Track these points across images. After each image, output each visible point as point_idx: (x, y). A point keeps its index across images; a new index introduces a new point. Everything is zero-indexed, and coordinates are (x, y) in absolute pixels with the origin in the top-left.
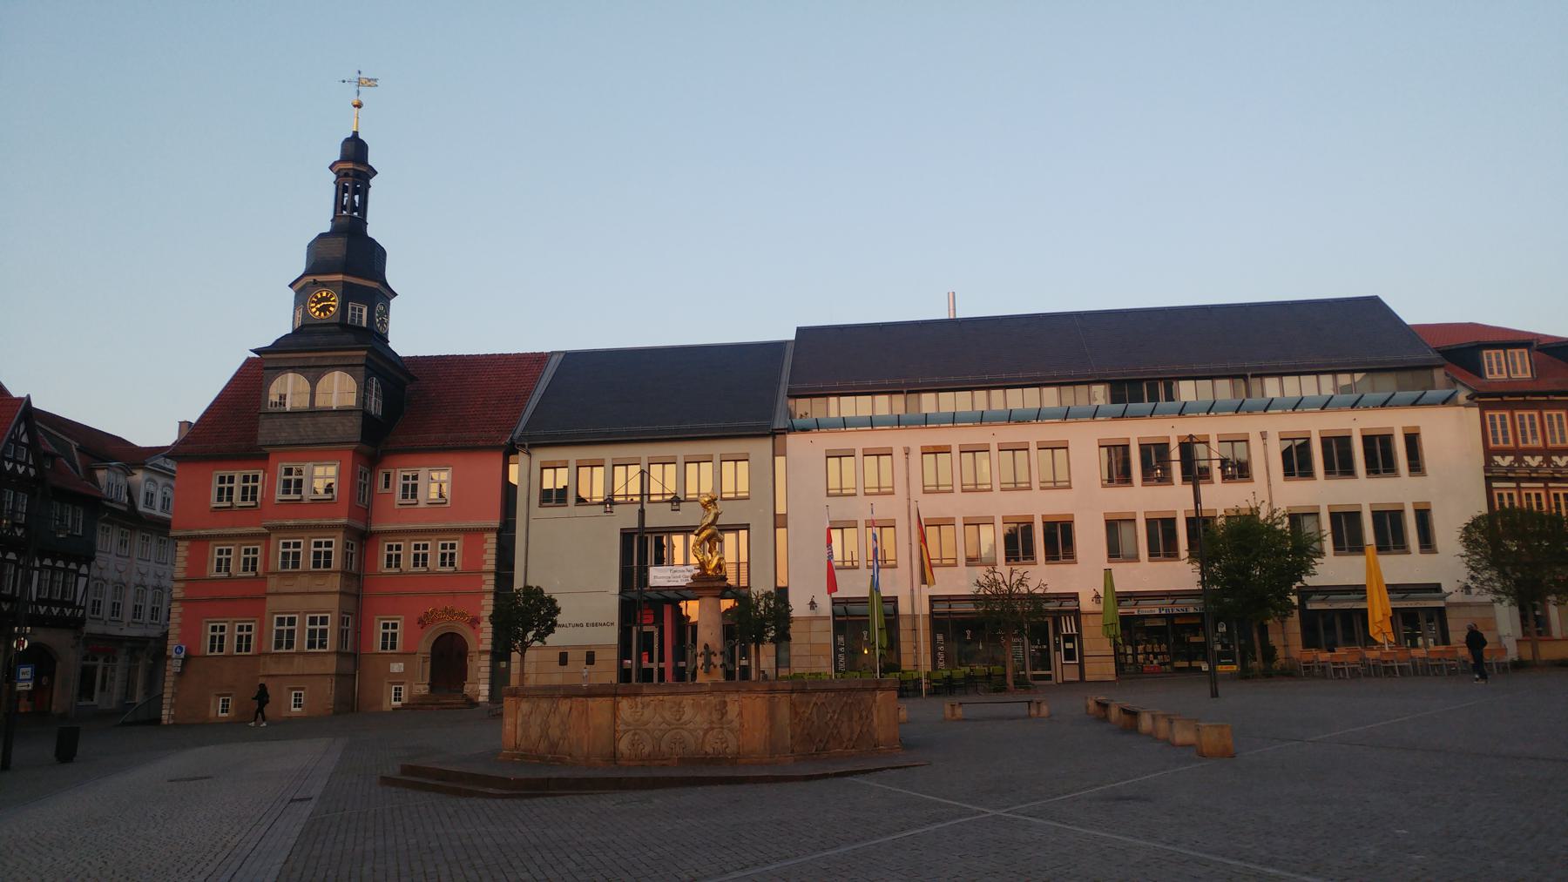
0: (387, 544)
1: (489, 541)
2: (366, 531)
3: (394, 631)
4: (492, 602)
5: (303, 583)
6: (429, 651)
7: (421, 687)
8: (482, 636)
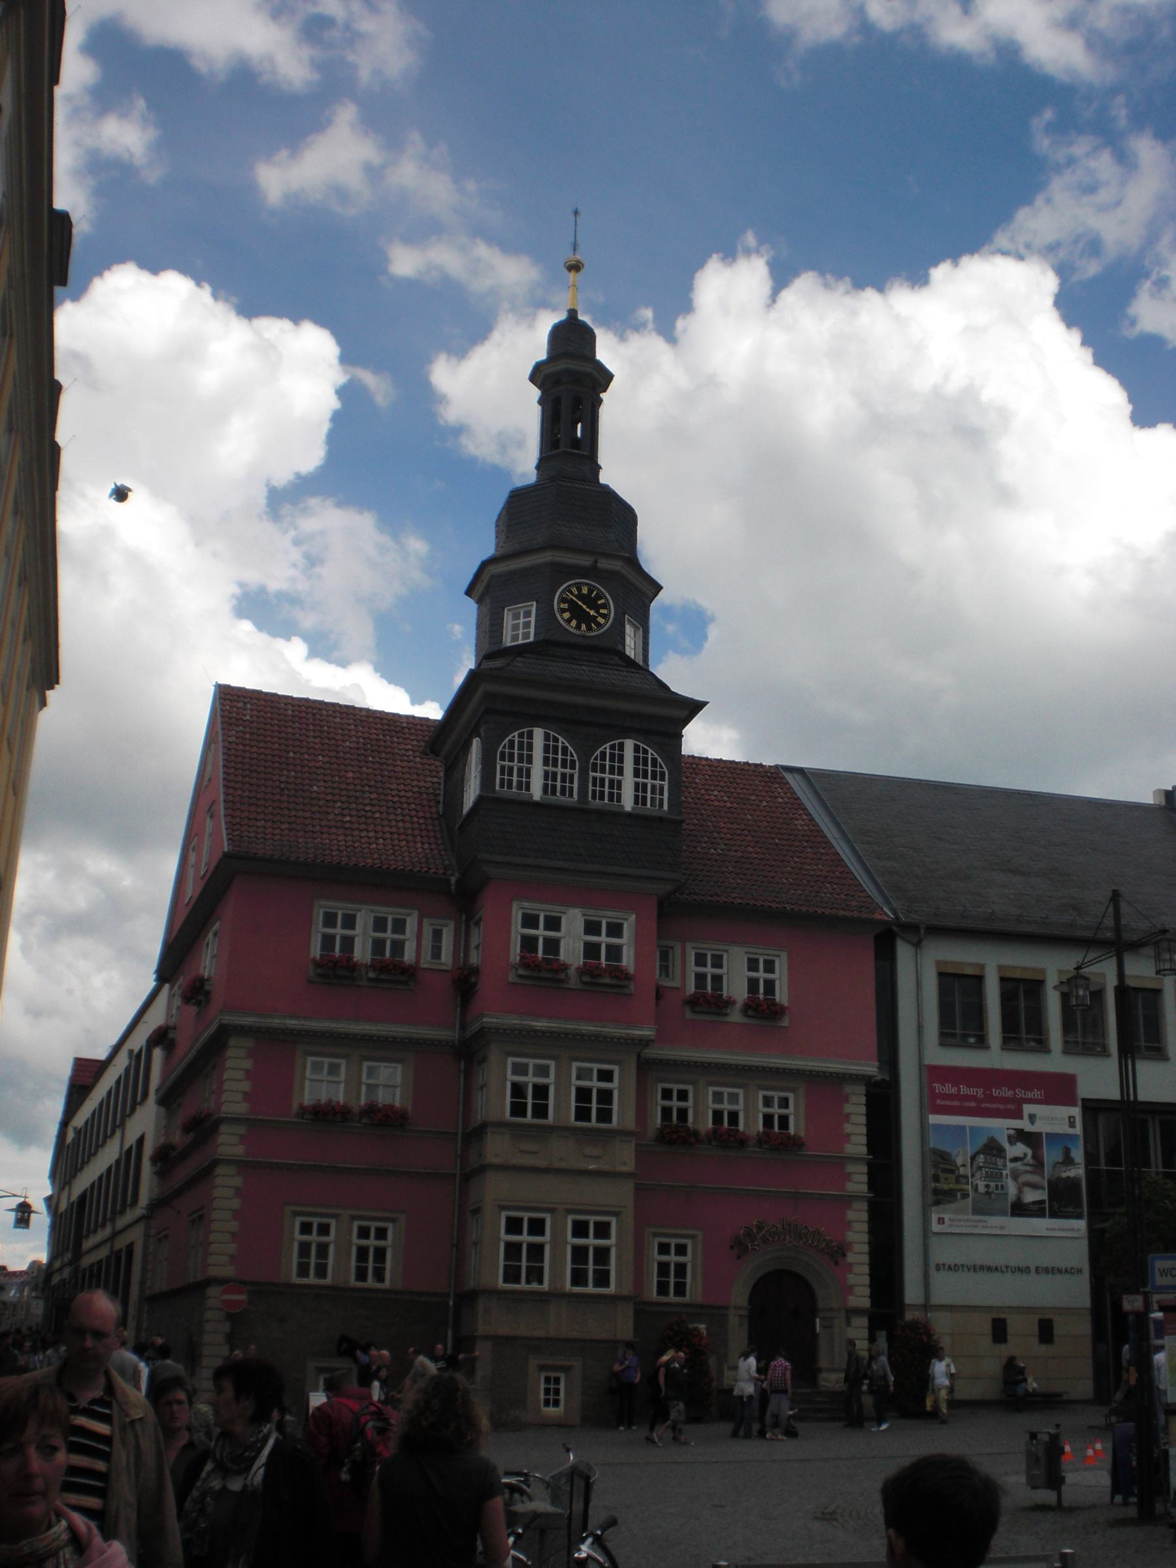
0: (660, 1086)
1: (854, 1099)
5: (563, 1152)
8: (852, 1279)
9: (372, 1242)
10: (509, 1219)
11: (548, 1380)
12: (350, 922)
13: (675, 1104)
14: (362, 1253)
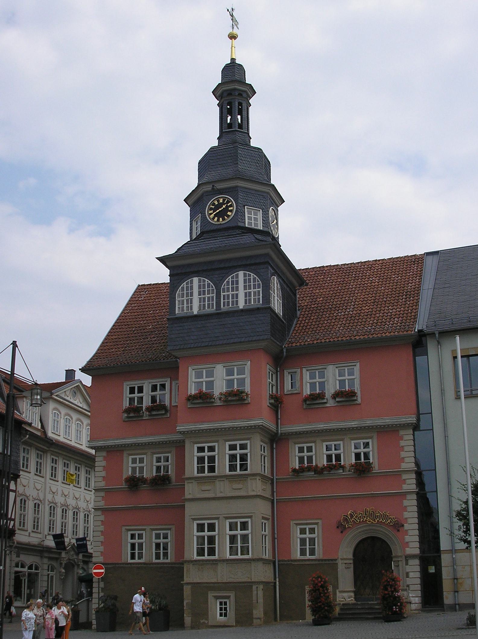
0: (297, 446)
1: (406, 437)
2: (277, 433)
3: (312, 536)
4: (415, 503)
6: (351, 556)
7: (345, 595)
9: (136, 541)
10: (198, 525)
11: (221, 603)
12: (141, 390)
13: (305, 454)
14: (158, 546)
